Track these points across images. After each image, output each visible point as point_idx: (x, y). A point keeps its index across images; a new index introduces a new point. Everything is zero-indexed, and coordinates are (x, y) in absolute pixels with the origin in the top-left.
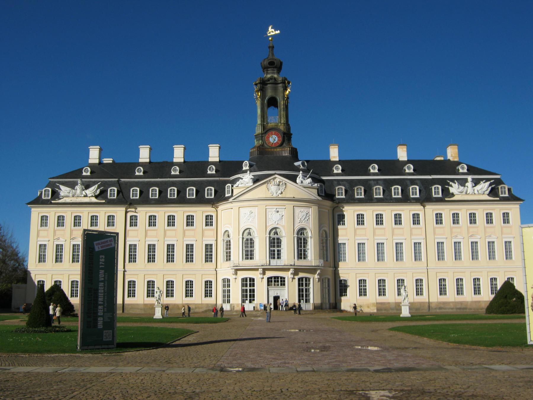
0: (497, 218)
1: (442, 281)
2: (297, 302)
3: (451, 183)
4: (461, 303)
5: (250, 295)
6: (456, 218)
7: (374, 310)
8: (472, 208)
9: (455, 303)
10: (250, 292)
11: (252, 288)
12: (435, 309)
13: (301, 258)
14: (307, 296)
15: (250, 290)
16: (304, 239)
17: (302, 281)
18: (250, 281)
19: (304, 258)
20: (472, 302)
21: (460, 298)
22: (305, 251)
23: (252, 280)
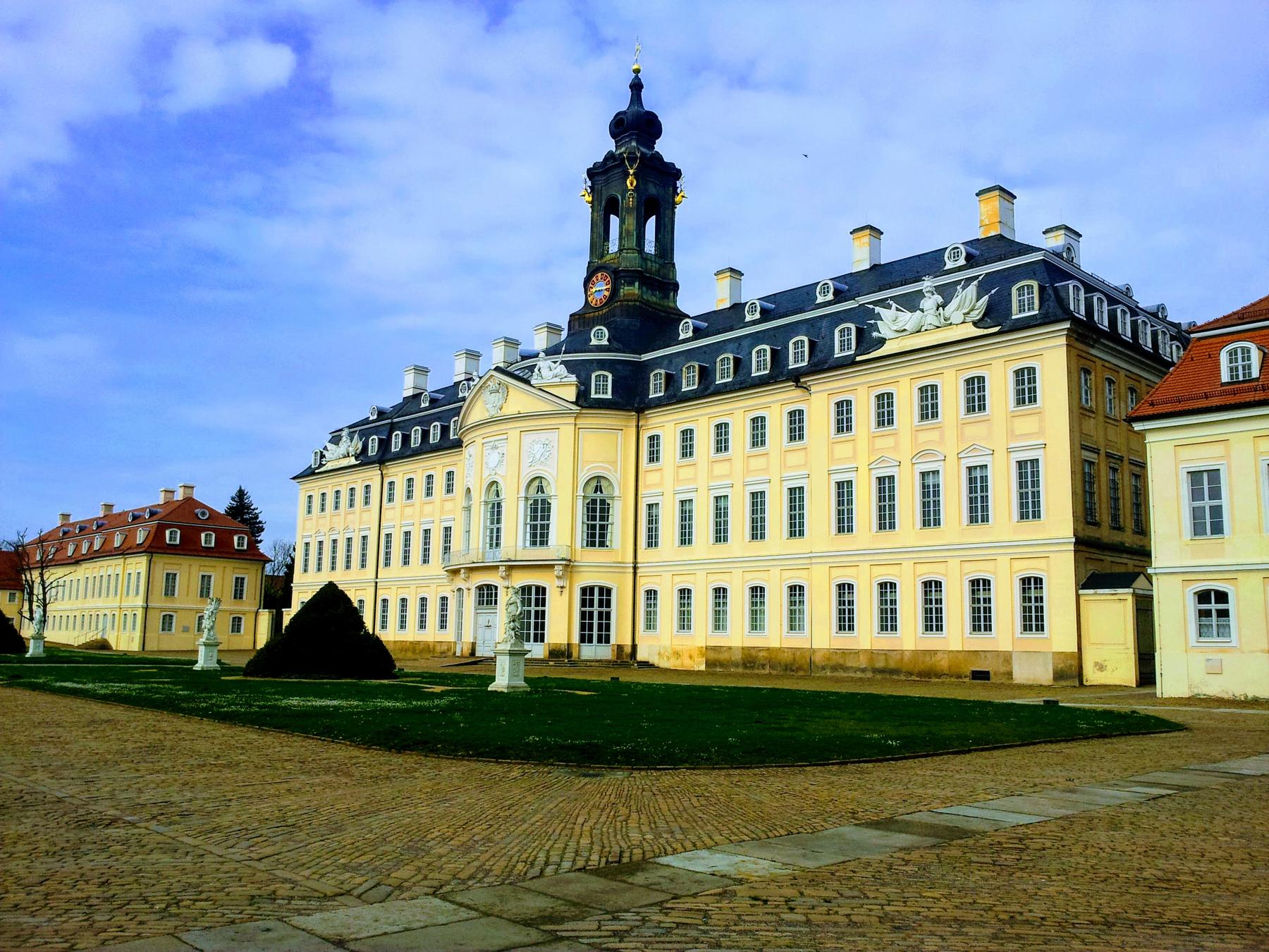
0: (1000, 389)
1: (845, 590)
2: (576, 639)
3: (877, 309)
4: (886, 653)
5: (536, 624)
6: (885, 412)
7: (699, 664)
8: (924, 372)
9: (871, 653)
10: (536, 617)
11: (540, 608)
12: (823, 668)
13: (593, 544)
14: (605, 627)
15: (537, 612)
16: (603, 502)
17: (592, 594)
18: (537, 593)
19: (602, 544)
20: (915, 652)
21: (886, 642)
22: (603, 528)
23: (541, 591)
